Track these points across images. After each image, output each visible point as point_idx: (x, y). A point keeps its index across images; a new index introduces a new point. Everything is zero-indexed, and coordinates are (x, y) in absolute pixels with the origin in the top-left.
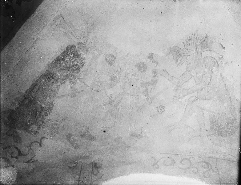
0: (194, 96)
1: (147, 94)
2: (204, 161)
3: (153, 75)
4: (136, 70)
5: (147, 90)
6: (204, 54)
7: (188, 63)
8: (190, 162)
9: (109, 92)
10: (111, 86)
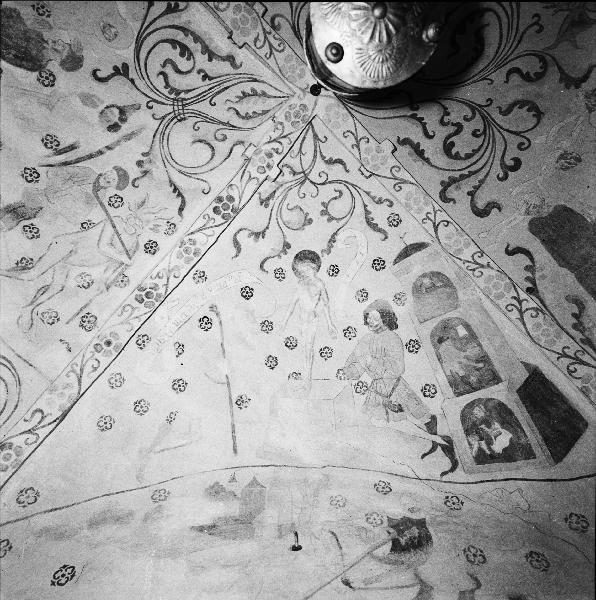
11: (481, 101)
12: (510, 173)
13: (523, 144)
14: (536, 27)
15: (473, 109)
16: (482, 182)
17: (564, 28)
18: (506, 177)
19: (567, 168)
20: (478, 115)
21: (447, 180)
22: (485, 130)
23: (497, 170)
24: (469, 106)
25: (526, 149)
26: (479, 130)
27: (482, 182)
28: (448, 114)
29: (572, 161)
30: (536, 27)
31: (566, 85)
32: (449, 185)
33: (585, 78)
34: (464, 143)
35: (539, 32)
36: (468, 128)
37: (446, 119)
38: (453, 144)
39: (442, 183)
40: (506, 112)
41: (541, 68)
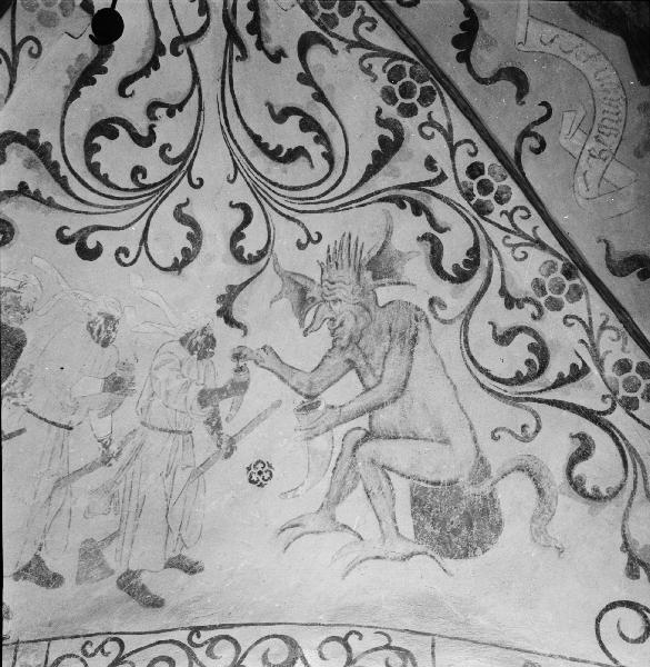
0: (359, 428)
1: (219, 426)
2: (392, 644)
3: (234, 365)
4: (183, 353)
5: (215, 414)
6: (385, 294)
7: (337, 323)
8: (348, 647)
9: (103, 427)
10: (109, 410)
11: (195, 174)
12: (73, 245)
13: (127, 255)
14: (304, 241)
15: (183, 157)
16: (50, 203)
17: (298, 279)
18: (65, 241)
19: (92, 331)
20: (177, 166)
21: (42, 141)
22: (144, 187)
23: (75, 224)
24: (190, 148)
25: (119, 261)
26: (144, 177)
27: (50, 203)
28: (171, 114)
29: (103, 335)
30: (304, 241)
31: (223, 296)
32: (33, 146)
33: (230, 321)
34: (117, 157)
35: (300, 246)
36: (149, 158)
37: (161, 112)
38: (113, 135)
39: (34, 133)
40: (180, 216)
41: (250, 255)
